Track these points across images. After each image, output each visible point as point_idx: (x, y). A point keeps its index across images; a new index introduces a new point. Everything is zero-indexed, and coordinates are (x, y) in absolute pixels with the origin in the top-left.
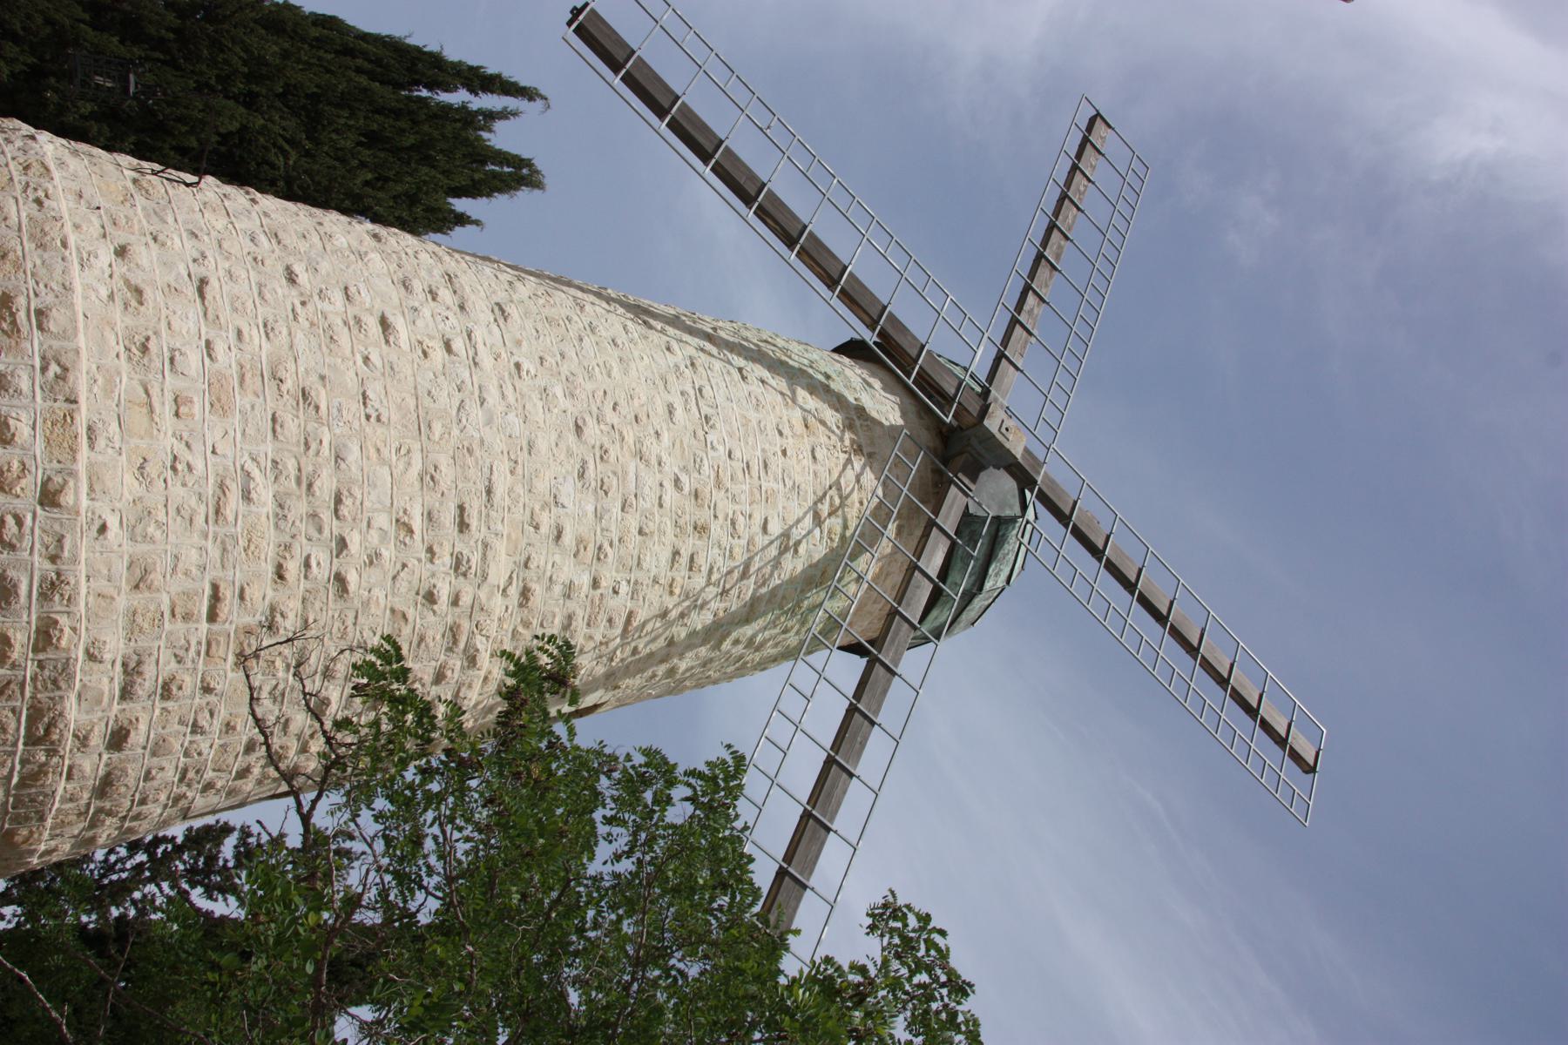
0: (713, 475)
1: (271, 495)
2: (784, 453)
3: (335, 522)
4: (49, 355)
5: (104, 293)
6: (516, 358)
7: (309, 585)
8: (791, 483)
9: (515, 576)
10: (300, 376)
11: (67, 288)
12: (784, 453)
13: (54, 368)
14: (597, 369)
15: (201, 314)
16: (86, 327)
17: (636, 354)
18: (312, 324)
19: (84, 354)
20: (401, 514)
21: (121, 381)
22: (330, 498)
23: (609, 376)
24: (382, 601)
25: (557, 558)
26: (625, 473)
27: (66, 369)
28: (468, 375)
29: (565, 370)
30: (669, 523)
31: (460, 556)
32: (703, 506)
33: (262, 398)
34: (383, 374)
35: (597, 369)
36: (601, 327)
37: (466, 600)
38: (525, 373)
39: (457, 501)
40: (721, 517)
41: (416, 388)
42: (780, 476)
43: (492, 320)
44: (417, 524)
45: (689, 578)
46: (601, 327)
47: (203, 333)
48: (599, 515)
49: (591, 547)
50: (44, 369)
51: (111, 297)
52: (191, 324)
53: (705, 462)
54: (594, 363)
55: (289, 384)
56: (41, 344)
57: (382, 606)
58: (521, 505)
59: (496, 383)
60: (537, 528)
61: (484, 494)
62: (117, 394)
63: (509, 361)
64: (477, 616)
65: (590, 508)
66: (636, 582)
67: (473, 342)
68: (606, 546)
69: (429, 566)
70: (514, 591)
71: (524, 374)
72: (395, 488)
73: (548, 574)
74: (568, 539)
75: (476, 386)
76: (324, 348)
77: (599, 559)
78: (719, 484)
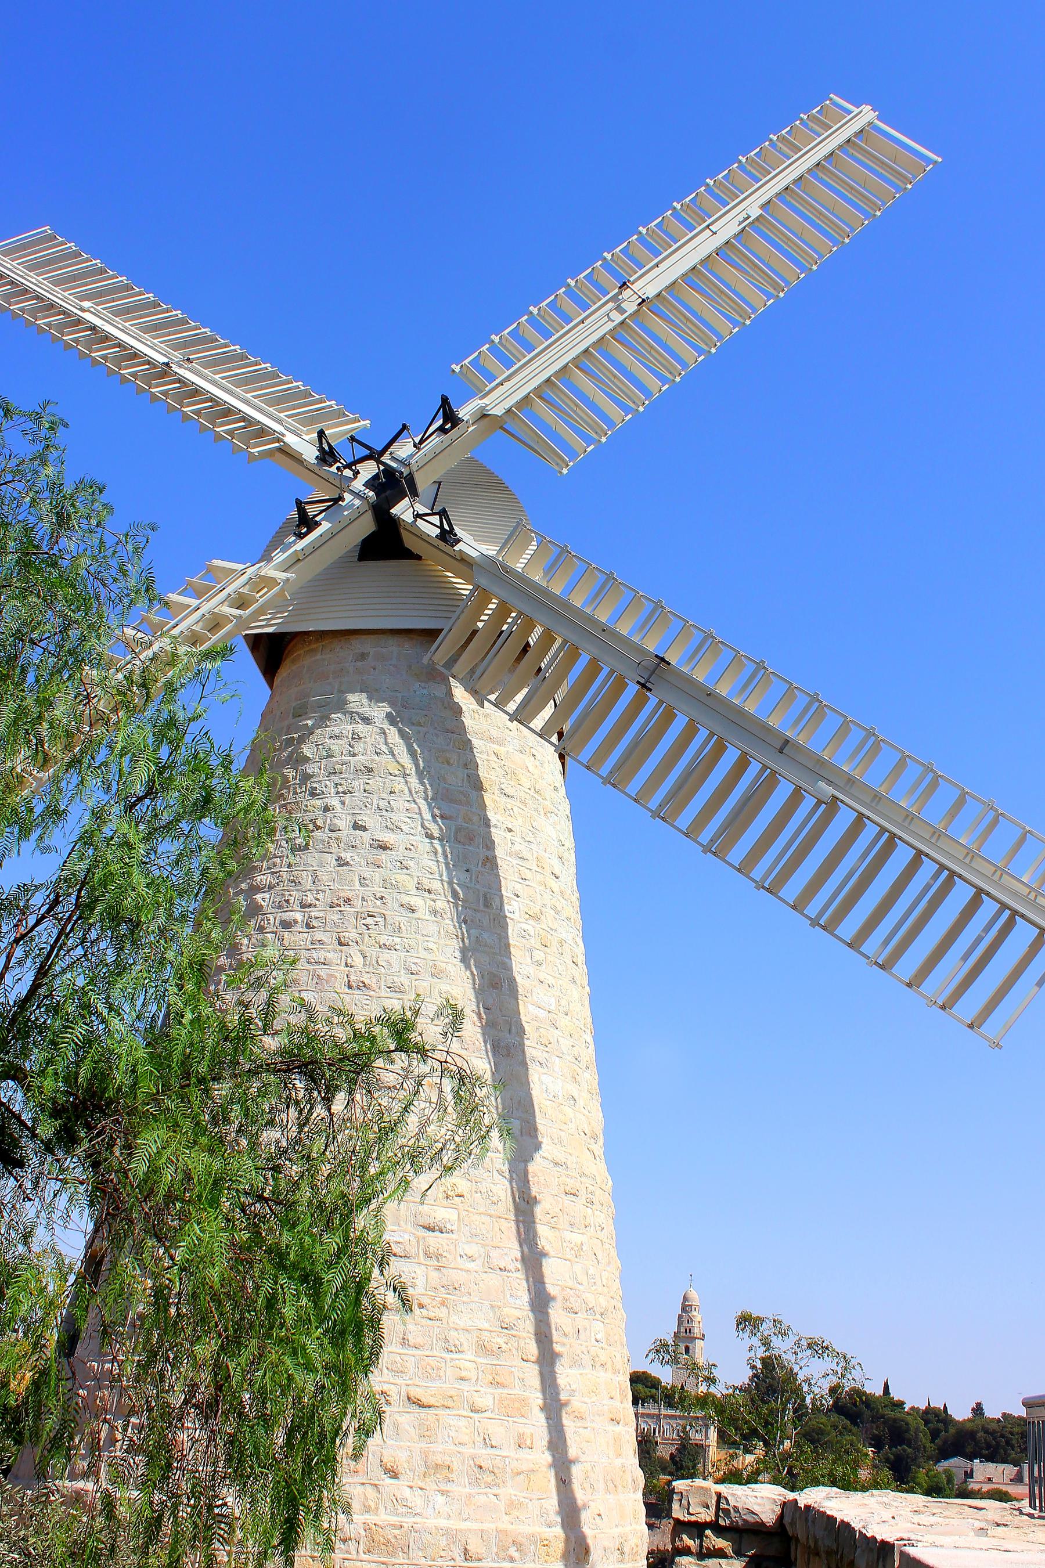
1: (569, 1371)
2: (510, 830)
3: (579, 1315)
4: (502, 1554)
5: (440, 1499)
7: (604, 1341)
10: (491, 1329)
11: (446, 1532)
12: (510, 830)
13: (513, 1551)
15: (448, 1411)
16: (476, 1520)
17: (423, 954)
18: (443, 1304)
19: (501, 1526)
21: (515, 1496)
22: (569, 1317)
27: (514, 1543)
33: (513, 1369)
41: (491, 1216)
47: (465, 1413)
48: (561, 1055)
50: (512, 1559)
51: (442, 1493)
52: (460, 1423)
55: (501, 1341)
56: (493, 1560)
62: (523, 1500)
72: (559, 1256)
76: (465, 1299)
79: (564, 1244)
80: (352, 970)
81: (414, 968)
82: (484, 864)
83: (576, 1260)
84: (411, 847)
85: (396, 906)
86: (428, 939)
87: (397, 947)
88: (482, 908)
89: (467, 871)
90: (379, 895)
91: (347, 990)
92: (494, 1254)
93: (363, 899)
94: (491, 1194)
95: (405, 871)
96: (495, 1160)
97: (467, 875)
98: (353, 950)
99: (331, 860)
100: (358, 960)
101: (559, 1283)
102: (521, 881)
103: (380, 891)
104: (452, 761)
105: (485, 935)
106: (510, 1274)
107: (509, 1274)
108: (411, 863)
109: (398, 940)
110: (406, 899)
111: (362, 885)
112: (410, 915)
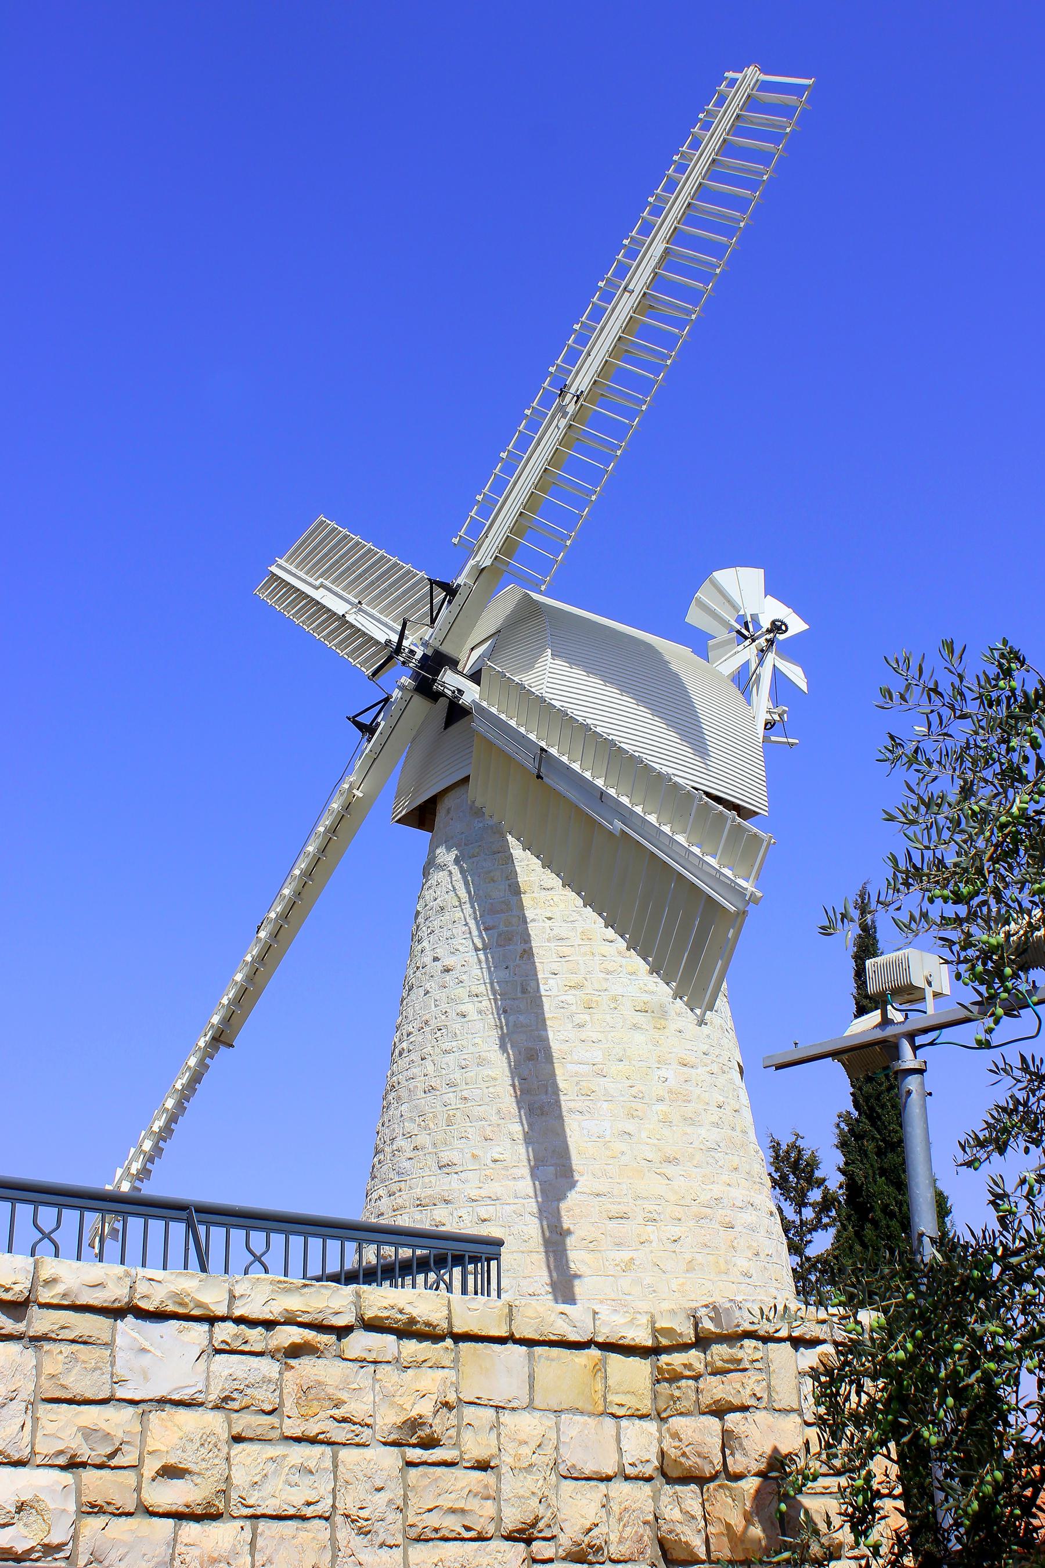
0: (573, 992)
2: (550, 919)
6: (489, 1162)
8: (574, 914)
9: (658, 1171)
12: (550, 919)
14: (491, 1090)
17: (472, 1049)
20: (619, 1268)
23: (495, 1079)
24: (682, 1280)
25: (644, 1135)
26: (576, 1074)
28: (508, 1206)
29: (495, 1119)
30: (612, 1034)
31: (646, 1219)
32: (597, 1002)
34: (514, 1278)
35: (491, 1090)
36: (452, 1076)
37: (678, 1212)
38: (501, 1156)
39: (607, 1222)
40: (605, 986)
42: (569, 925)
43: (455, 1176)
44: (625, 1255)
45: (653, 1012)
46: (452, 1076)
48: (610, 1098)
49: (633, 1105)
53: (563, 998)
54: (486, 1090)
57: (684, 1280)
58: (606, 1167)
59: (511, 1183)
60: (623, 1153)
61: (600, 1199)
63: (493, 1169)
64: (688, 1201)
65: (605, 1105)
66: (659, 1062)
67: (480, 1199)
68: (633, 1091)
69: (654, 1244)
70: (670, 1170)
71: (501, 1157)
73: (656, 1141)
74: (630, 1126)
75: (516, 1201)
77: (643, 1098)
78: (579, 987)
79: (607, 1263)
80: (426, 1078)
81: (463, 1063)
82: (521, 957)
83: (624, 1274)
84: (465, 963)
85: (454, 1014)
86: (475, 1035)
87: (454, 1050)
88: (519, 995)
89: (507, 968)
90: (444, 1011)
91: (424, 1096)
92: (524, 1283)
93: (436, 1018)
94: (522, 1234)
95: (461, 984)
96: (526, 1205)
97: (507, 971)
98: (428, 1063)
99: (421, 991)
100: (430, 1069)
101: (596, 1297)
102: (560, 960)
103: (444, 1006)
104: (495, 879)
105: (522, 1018)
106: (542, 1297)
107: (539, 1298)
108: (464, 977)
109: (454, 1044)
110: (462, 1008)
111: (436, 1006)
112: (463, 1020)
